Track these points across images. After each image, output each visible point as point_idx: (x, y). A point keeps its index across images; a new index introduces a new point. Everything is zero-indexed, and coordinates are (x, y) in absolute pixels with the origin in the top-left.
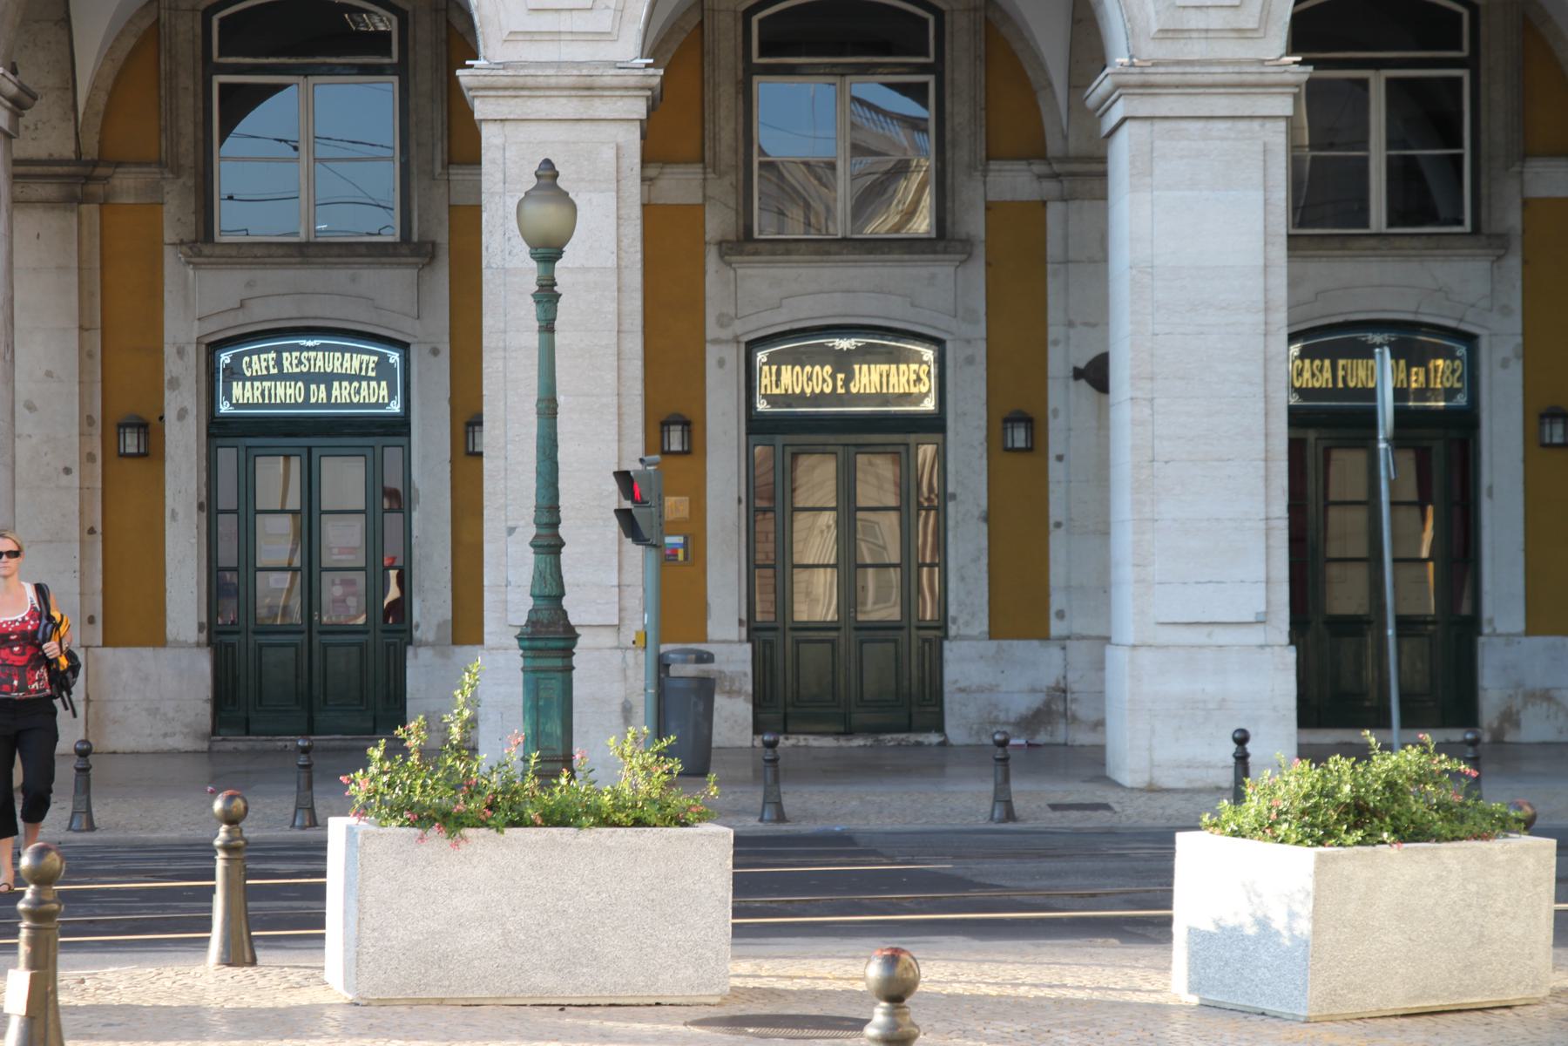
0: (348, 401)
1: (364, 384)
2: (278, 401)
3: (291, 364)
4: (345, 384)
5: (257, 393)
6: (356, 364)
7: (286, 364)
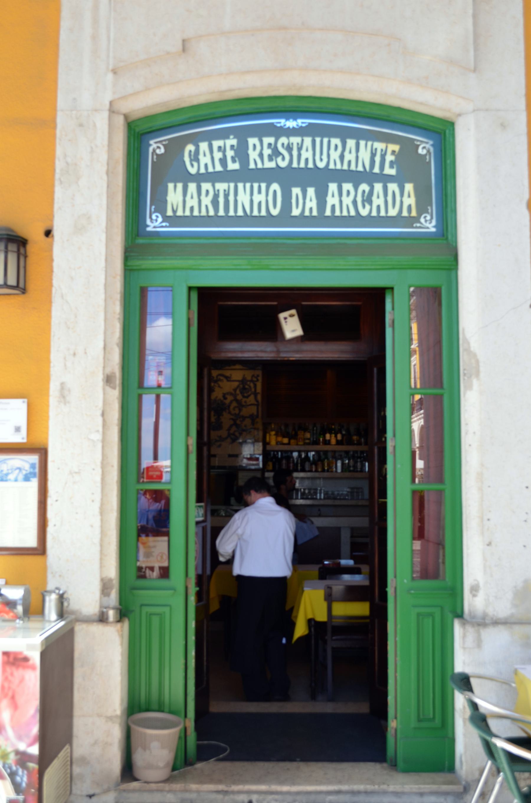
0: (353, 213)
1: (378, 187)
2: (240, 213)
3: (261, 155)
4: (347, 186)
5: (207, 201)
6: (365, 155)
7: (253, 155)
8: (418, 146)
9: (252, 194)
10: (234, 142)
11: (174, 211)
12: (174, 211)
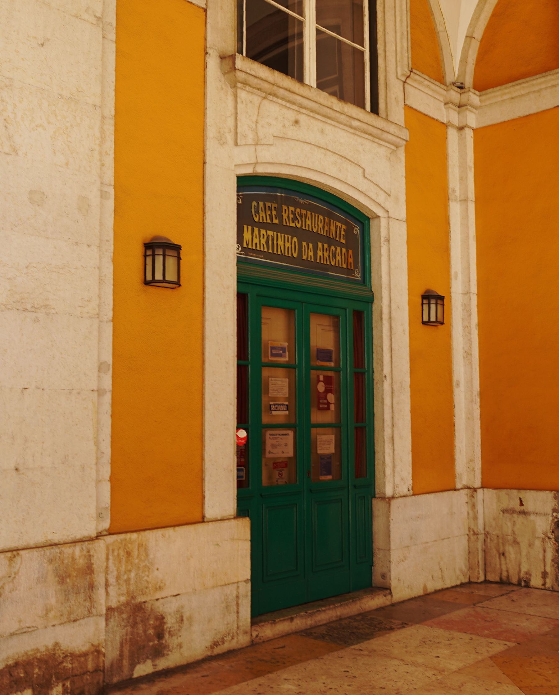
5: (263, 241)
8: (354, 228)
9: (284, 242)
10: (276, 205)
11: (247, 245)
12: (247, 245)
